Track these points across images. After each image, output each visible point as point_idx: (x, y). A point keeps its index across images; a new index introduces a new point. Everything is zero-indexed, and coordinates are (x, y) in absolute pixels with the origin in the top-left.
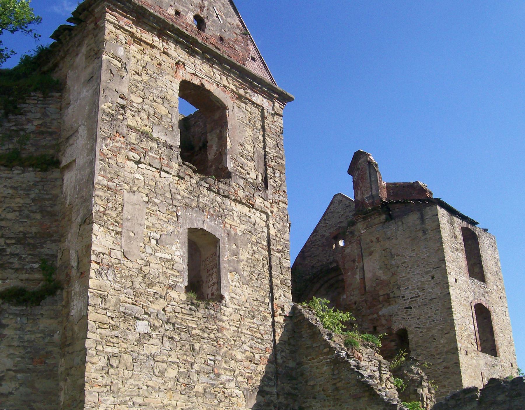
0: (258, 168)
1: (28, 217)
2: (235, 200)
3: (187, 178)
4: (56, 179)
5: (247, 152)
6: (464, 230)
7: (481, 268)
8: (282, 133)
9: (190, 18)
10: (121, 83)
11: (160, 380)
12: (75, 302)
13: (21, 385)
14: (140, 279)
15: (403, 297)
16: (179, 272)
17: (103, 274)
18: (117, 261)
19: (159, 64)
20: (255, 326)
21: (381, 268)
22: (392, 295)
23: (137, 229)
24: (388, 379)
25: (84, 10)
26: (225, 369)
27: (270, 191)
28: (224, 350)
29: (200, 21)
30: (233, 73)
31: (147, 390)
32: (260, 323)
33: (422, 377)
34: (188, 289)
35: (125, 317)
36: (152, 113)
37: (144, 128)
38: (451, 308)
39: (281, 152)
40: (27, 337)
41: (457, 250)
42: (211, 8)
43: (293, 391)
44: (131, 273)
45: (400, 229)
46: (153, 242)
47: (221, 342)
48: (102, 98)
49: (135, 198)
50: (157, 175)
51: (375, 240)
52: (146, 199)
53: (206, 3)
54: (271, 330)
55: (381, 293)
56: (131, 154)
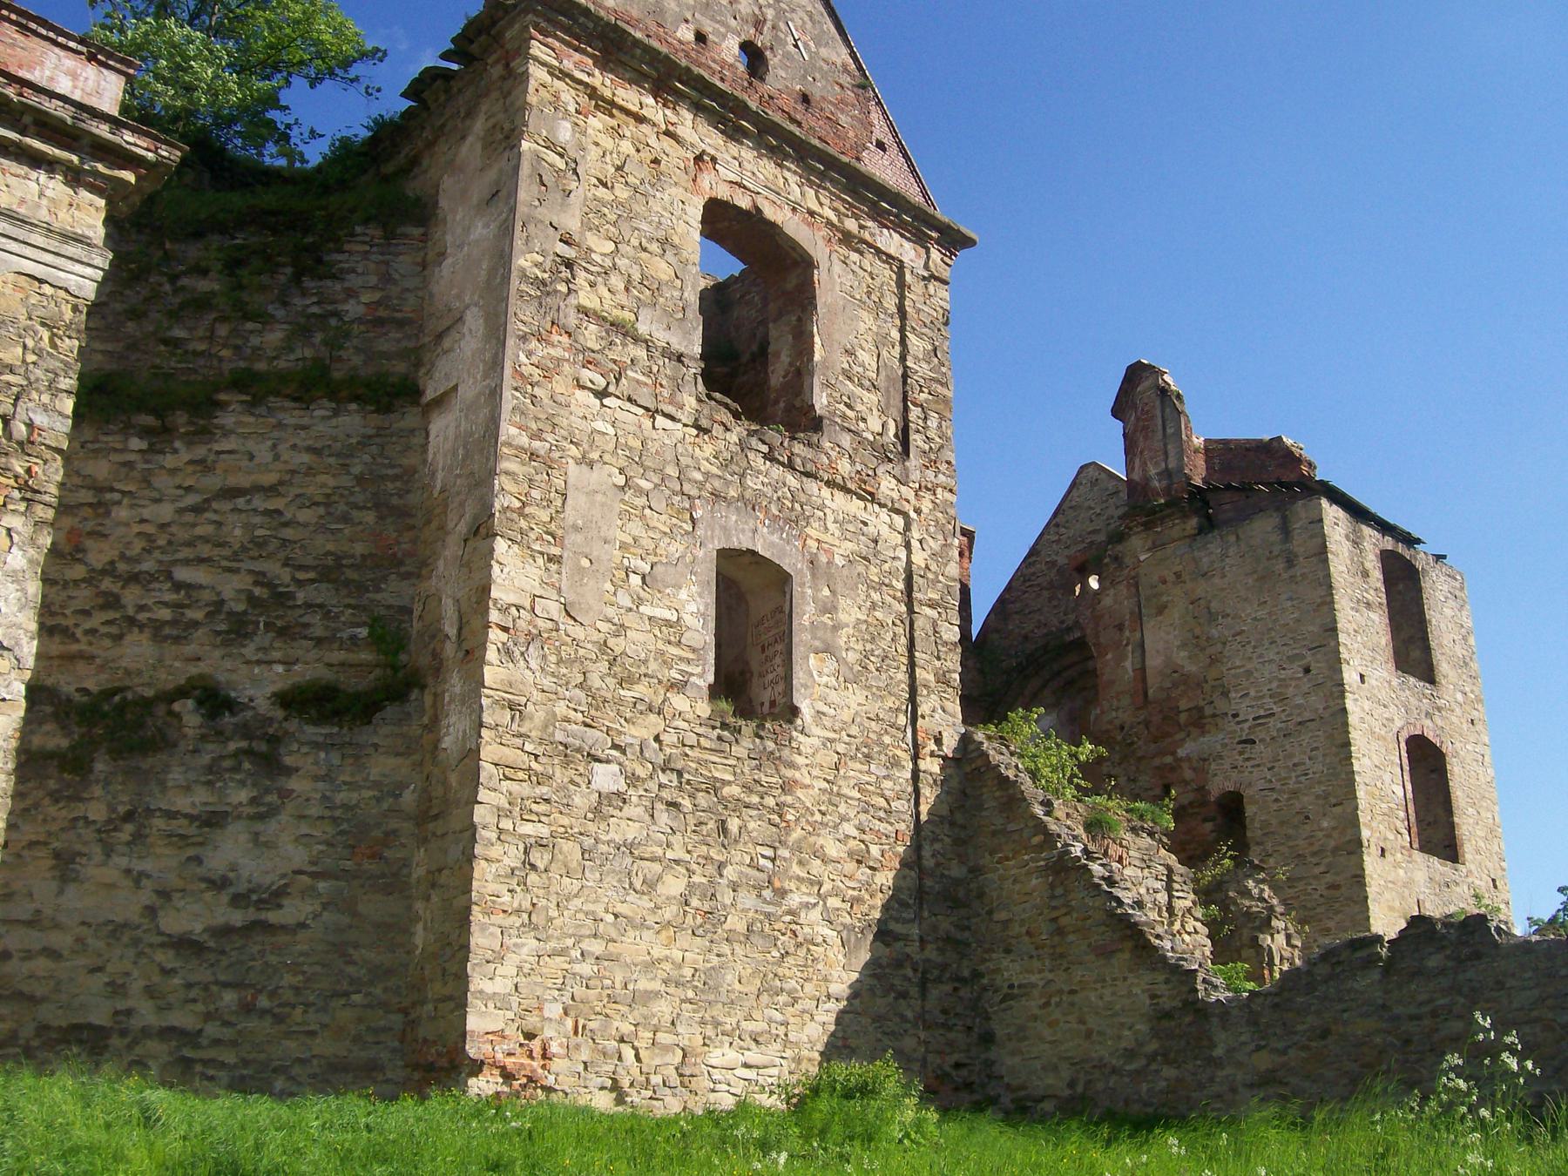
0: (888, 404)
1: (345, 519)
2: (829, 484)
3: (717, 430)
4: (412, 431)
5: (860, 370)
6: (1387, 558)
7: (1427, 649)
8: (946, 324)
9: (729, 49)
10: (564, 206)
11: (645, 902)
12: (453, 719)
13: (325, 906)
14: (603, 666)
15: (1235, 716)
16: (694, 650)
17: (517, 653)
18: (550, 625)
19: (656, 161)
20: (873, 779)
21: (1184, 645)
22: (1208, 711)
23: (597, 550)
24: (1189, 910)
25: (480, 33)
26: (799, 878)
27: (914, 461)
28: (797, 834)
29: (754, 57)
30: (832, 180)
31: (614, 925)
32: (884, 772)
33: (1271, 909)
34: (715, 692)
35: (566, 753)
36: (637, 276)
37: (617, 312)
38: (1348, 744)
39: (944, 370)
40: (341, 797)
41: (1368, 605)
42: (782, 25)
43: (959, 936)
44: (581, 652)
45: (1231, 552)
46: (635, 580)
47: (789, 817)
48: (518, 243)
49: (597, 476)
50: (647, 423)
51: (1171, 578)
52: (621, 481)
53: (770, 13)
54: (910, 789)
55: (1183, 704)
56: (587, 375)
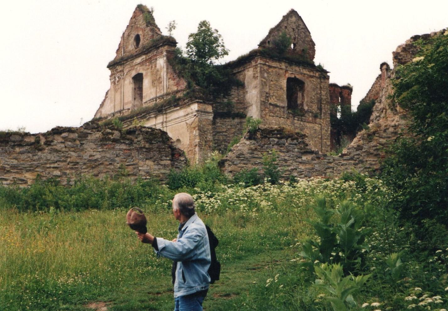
2: (308, 122)
27: (323, 115)
53: (297, 36)
